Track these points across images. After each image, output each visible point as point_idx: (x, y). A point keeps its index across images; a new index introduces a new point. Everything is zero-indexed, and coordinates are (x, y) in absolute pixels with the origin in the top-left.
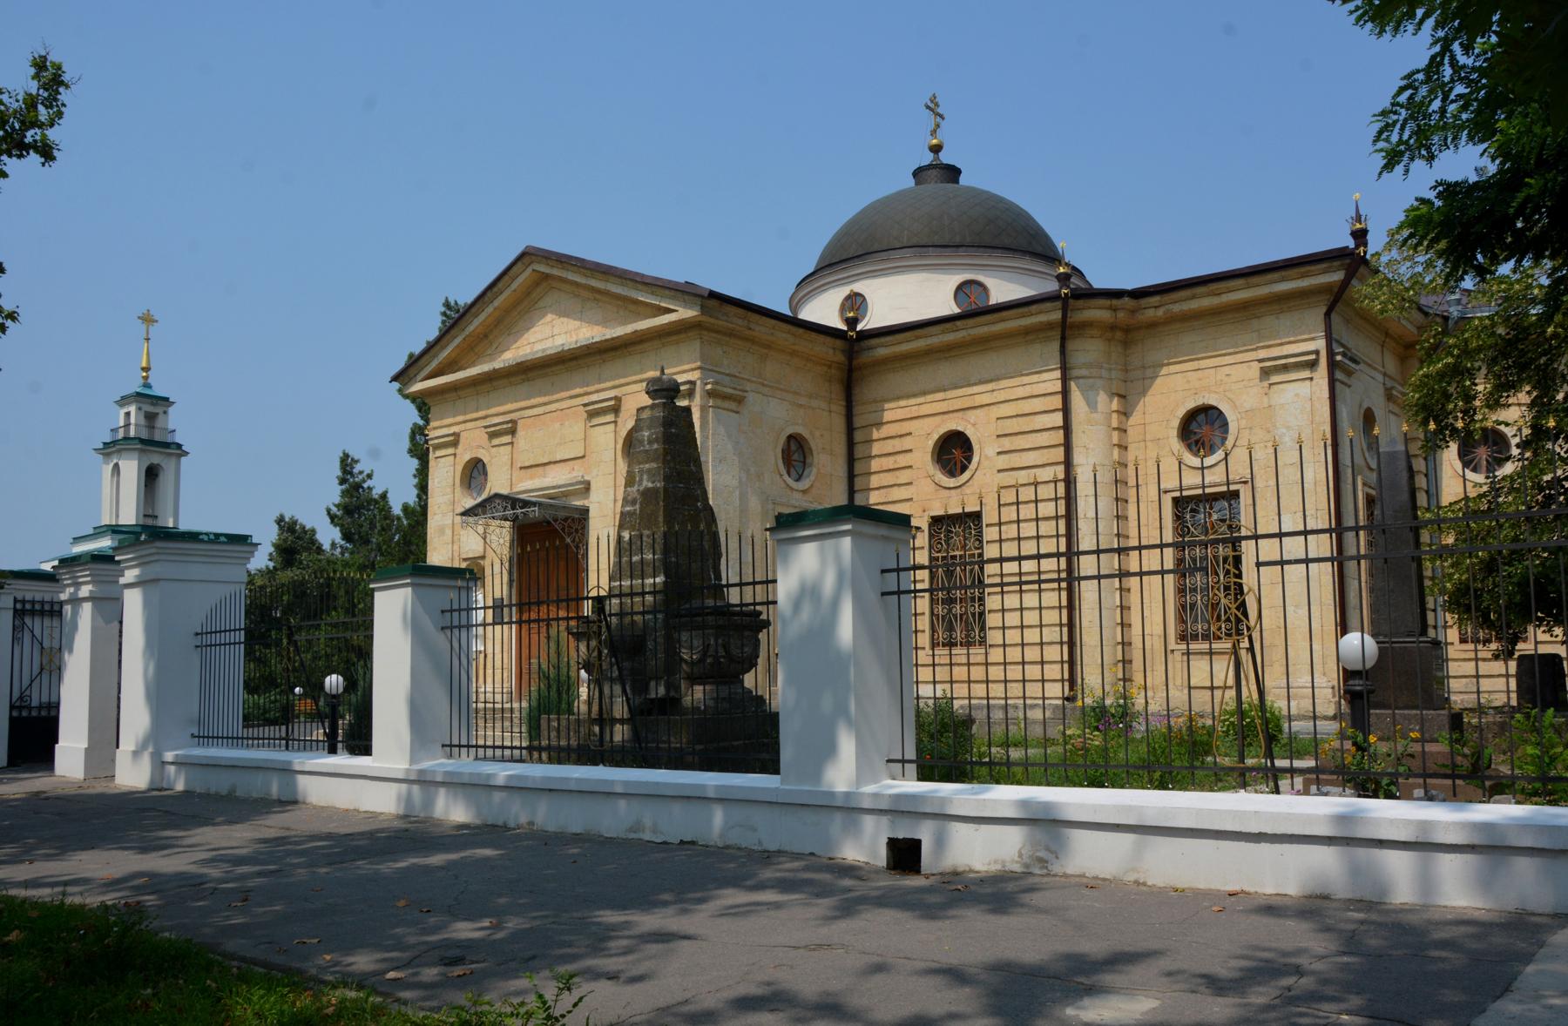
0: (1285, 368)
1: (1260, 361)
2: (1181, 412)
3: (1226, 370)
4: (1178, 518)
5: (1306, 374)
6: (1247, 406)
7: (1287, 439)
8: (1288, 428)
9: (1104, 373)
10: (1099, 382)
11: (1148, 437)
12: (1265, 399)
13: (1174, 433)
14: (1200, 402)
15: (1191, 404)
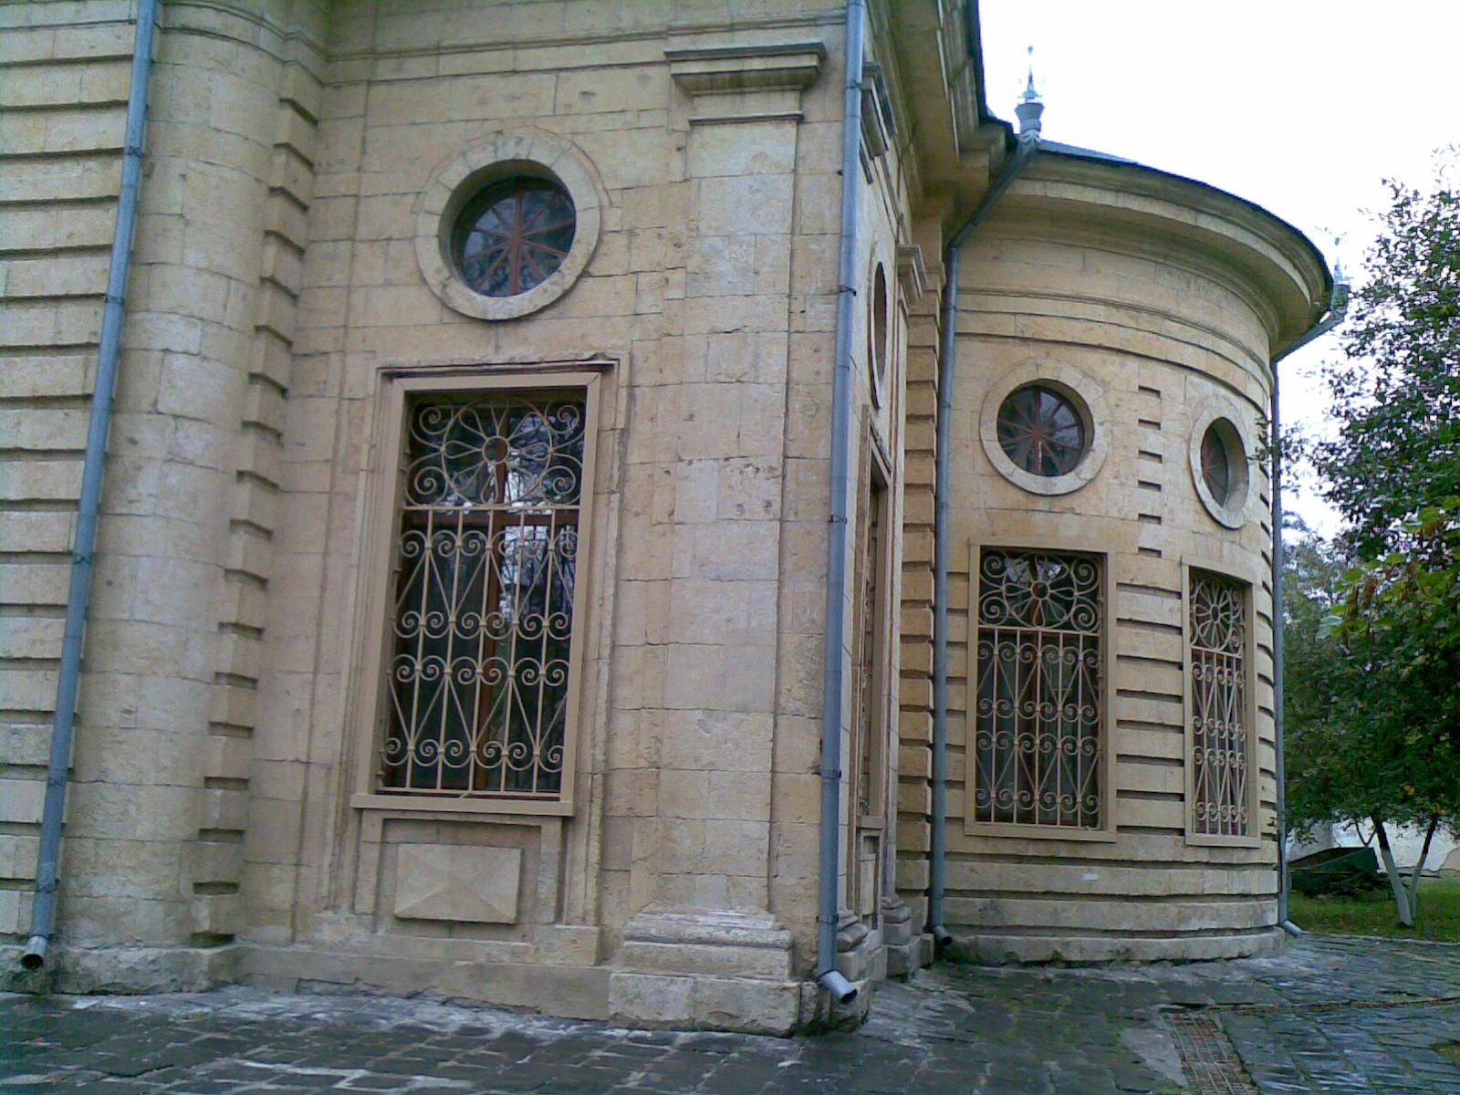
0: (737, 84)
1: (673, 57)
2: (457, 174)
3: (584, 81)
4: (416, 448)
5: (786, 104)
6: (628, 175)
7: (724, 267)
8: (730, 238)
9: (265, 38)
10: (248, 59)
11: (363, 231)
12: (677, 163)
13: (431, 226)
14: (508, 152)
15: (483, 158)
